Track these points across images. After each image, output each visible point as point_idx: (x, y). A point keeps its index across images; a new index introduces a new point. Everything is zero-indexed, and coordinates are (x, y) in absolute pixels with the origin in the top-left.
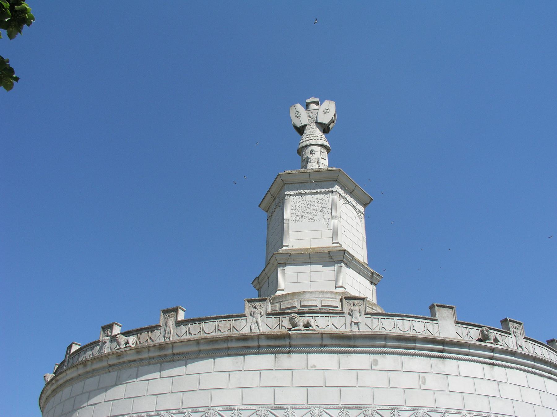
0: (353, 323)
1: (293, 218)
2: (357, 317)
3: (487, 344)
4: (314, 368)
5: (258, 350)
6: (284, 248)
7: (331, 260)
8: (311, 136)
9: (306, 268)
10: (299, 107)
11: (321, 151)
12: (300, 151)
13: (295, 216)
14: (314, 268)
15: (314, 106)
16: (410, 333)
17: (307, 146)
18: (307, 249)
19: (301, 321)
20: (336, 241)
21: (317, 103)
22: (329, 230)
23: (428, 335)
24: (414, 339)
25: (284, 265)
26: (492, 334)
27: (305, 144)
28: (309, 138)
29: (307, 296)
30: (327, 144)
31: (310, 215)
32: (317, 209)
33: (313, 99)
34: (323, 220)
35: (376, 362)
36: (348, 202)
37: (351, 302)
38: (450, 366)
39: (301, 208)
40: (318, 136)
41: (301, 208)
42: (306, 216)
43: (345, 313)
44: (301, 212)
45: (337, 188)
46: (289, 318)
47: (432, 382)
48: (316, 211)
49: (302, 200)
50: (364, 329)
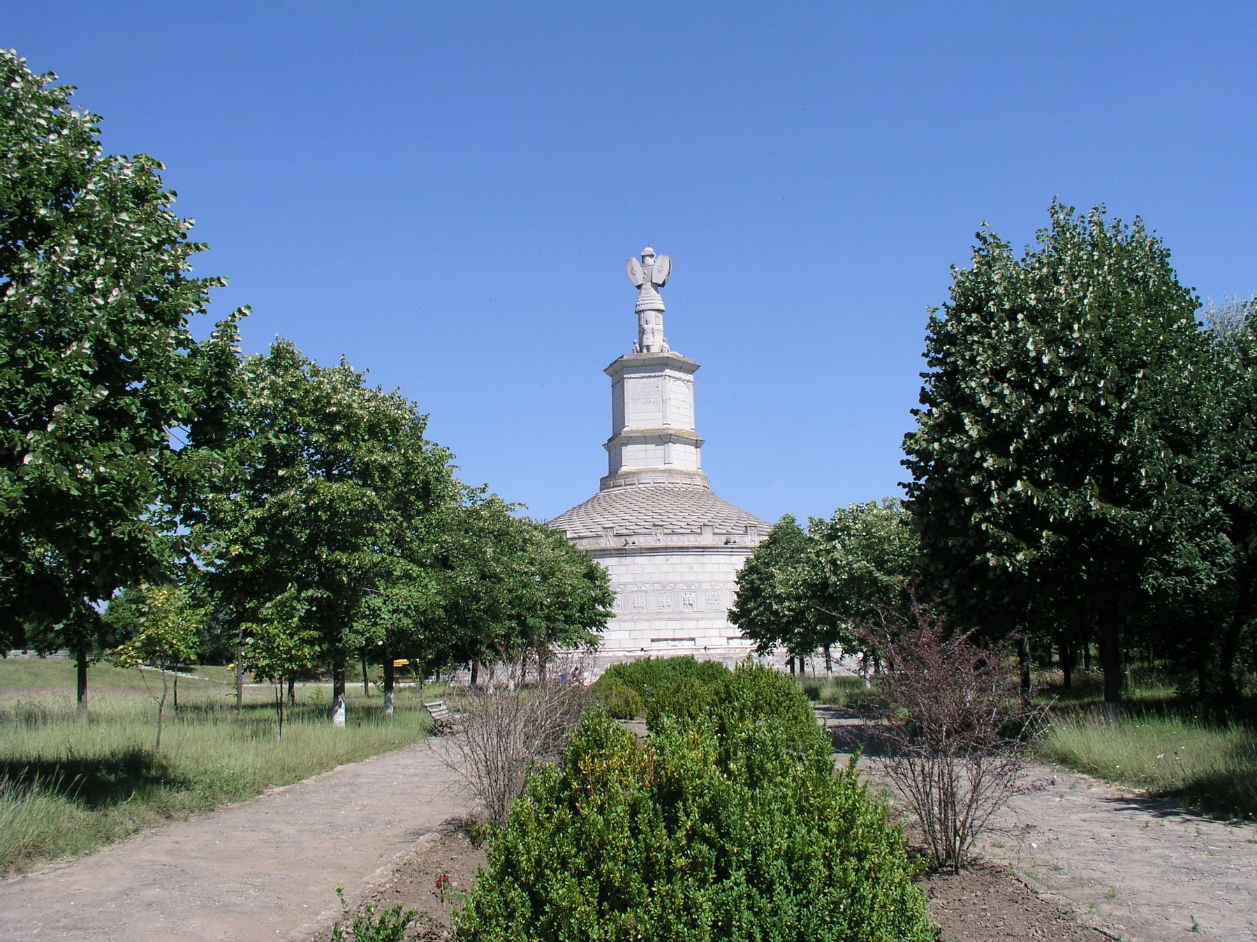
2: (660, 537)
3: (729, 546)
4: (638, 564)
5: (611, 556)
6: (626, 429)
9: (643, 446)
10: (635, 263)
12: (639, 312)
14: (650, 447)
15: (649, 261)
16: (686, 544)
17: (643, 311)
18: (643, 431)
19: (630, 540)
21: (652, 256)
23: (697, 544)
24: (688, 548)
25: (626, 445)
26: (733, 538)
27: (641, 308)
29: (643, 475)
30: (662, 307)
33: (649, 250)
35: (668, 560)
36: (680, 379)
38: (707, 559)
45: (668, 372)
47: (695, 569)
50: (662, 544)
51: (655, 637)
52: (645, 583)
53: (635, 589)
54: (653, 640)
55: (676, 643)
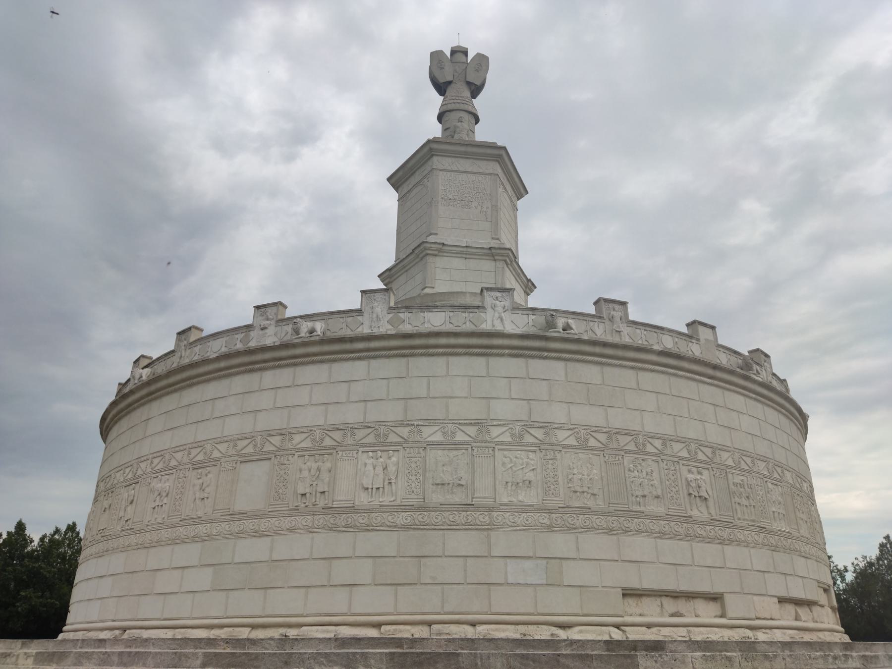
0: (614, 331)
1: (443, 200)
7: (492, 258)
8: (457, 98)
11: (469, 120)
13: (446, 198)
20: (497, 237)
22: (487, 221)
28: (455, 101)
31: (464, 200)
32: (474, 194)
34: (479, 208)
37: (611, 305)
39: (453, 189)
40: (467, 100)
41: (453, 189)
42: (460, 200)
43: (605, 318)
44: (454, 194)
46: (545, 318)
48: (471, 196)
49: (455, 179)
51: (634, 583)
52: (593, 430)
53: (572, 441)
54: (628, 594)
55: (681, 605)
